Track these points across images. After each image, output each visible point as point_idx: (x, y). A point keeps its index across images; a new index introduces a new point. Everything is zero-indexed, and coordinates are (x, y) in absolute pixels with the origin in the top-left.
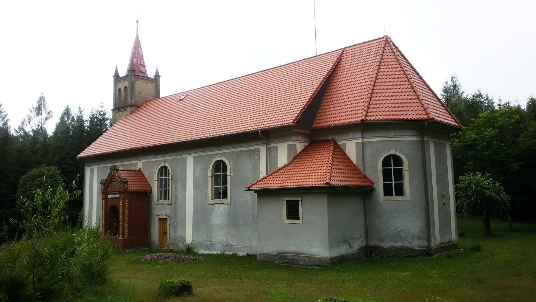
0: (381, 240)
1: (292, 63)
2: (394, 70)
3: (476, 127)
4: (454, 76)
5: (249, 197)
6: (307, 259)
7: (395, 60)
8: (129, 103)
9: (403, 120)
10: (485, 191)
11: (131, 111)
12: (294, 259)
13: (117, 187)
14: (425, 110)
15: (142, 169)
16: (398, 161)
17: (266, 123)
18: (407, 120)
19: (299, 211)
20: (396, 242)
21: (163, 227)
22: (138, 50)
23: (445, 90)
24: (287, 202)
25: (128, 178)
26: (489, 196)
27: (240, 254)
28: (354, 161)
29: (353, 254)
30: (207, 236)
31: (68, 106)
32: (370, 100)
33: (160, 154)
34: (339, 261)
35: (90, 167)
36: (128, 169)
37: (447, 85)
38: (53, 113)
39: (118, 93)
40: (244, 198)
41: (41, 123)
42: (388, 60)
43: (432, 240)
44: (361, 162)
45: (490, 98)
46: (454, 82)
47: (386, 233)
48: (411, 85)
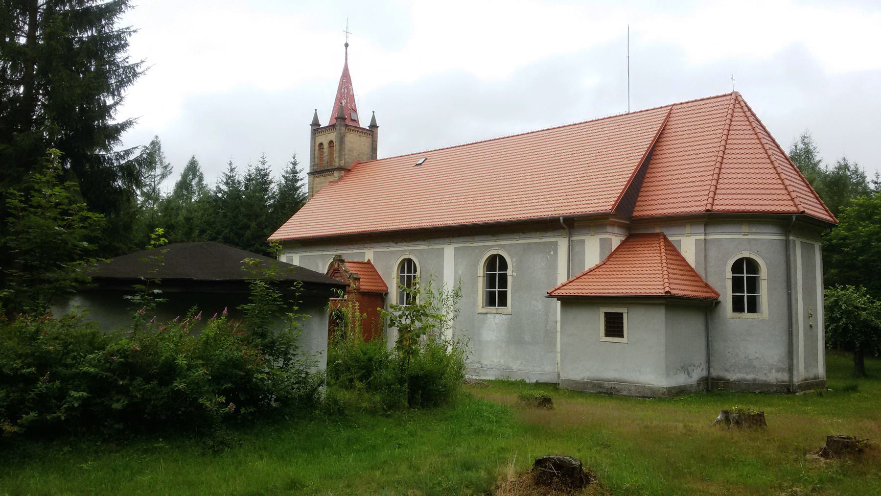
0: (726, 370)
1: (592, 121)
2: (749, 141)
3: (845, 218)
4: (806, 136)
6: (633, 388)
7: (750, 127)
8: (337, 165)
9: (763, 212)
10: (859, 312)
11: (339, 177)
12: (614, 388)
14: (792, 199)
15: (372, 262)
16: (752, 266)
17: (569, 208)
18: (769, 212)
19: (622, 327)
20: (747, 373)
22: (348, 88)
23: (793, 156)
24: (606, 314)
25: (359, 273)
26: (865, 321)
27: (528, 381)
28: (693, 266)
29: (691, 386)
31: (193, 158)
32: (717, 183)
33: (401, 242)
34: (677, 393)
35: (288, 255)
36: (351, 261)
37: (796, 151)
38: (172, 167)
39: (317, 149)
41: (154, 181)
42: (740, 128)
43: (795, 373)
44: (703, 265)
45: (860, 170)
46: (805, 144)
47: (733, 361)
48: (772, 164)
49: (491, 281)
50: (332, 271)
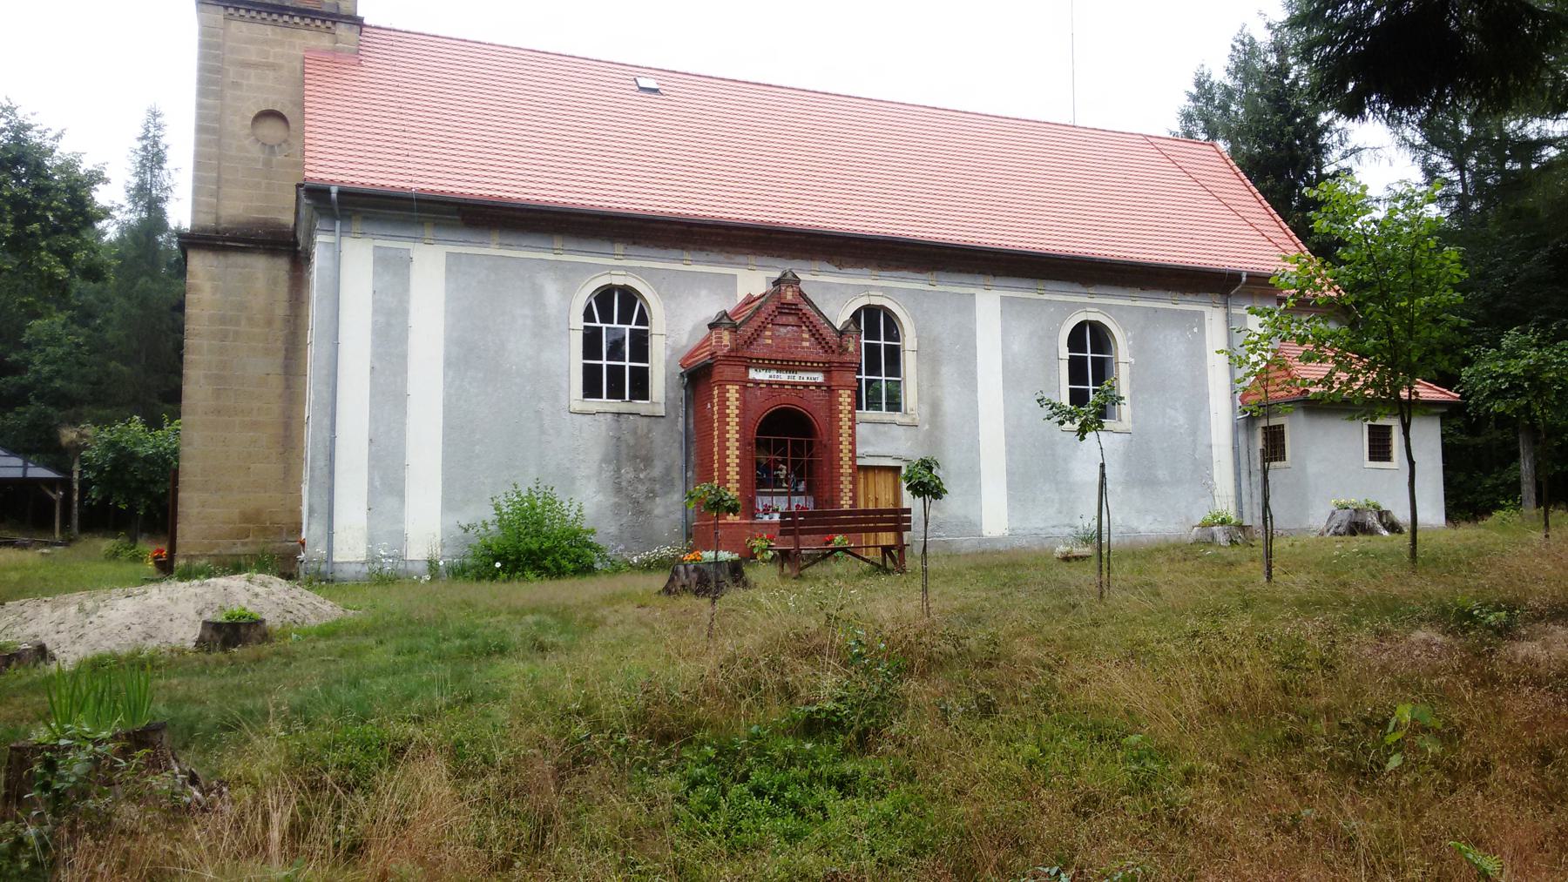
5: (1182, 421)
21: (871, 496)
35: (379, 243)
40: (1167, 421)
49: (1077, 370)
50: (771, 307)
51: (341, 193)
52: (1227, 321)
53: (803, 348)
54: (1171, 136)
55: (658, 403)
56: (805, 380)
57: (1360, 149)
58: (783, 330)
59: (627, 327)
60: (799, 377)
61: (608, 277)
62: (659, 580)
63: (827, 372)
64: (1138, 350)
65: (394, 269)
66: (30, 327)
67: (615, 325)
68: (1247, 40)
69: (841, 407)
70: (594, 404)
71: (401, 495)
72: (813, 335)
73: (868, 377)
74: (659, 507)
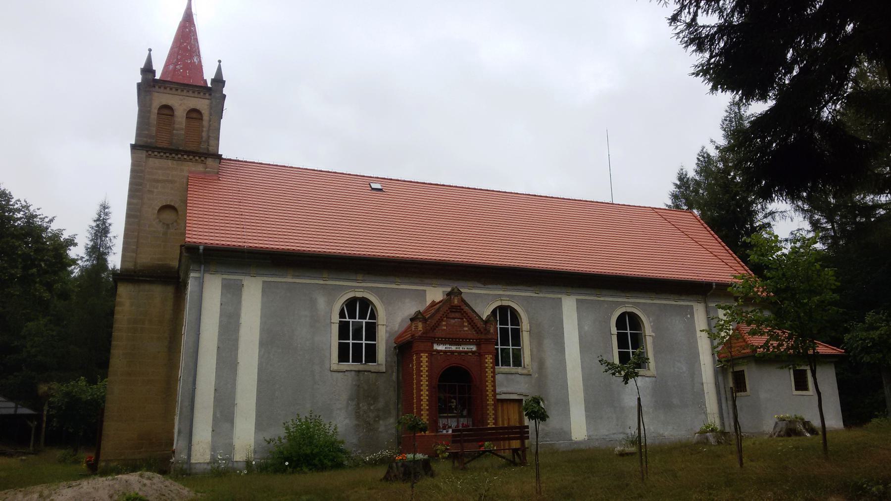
5: (684, 369)
13: (466, 330)
30: (617, 425)
35: (225, 276)
40: (677, 370)
49: (622, 341)
51: (204, 249)
52: (707, 311)
53: (464, 331)
54: (667, 208)
55: (382, 365)
56: (466, 350)
57: (775, 212)
58: (453, 321)
59: (364, 321)
60: (461, 348)
61: (353, 292)
62: (381, 472)
63: (478, 345)
64: (655, 329)
65: (233, 293)
66: (26, 326)
67: (357, 320)
68: (705, 155)
69: (487, 365)
70: (344, 366)
71: (232, 422)
72: (470, 324)
73: (502, 347)
74: (382, 426)
